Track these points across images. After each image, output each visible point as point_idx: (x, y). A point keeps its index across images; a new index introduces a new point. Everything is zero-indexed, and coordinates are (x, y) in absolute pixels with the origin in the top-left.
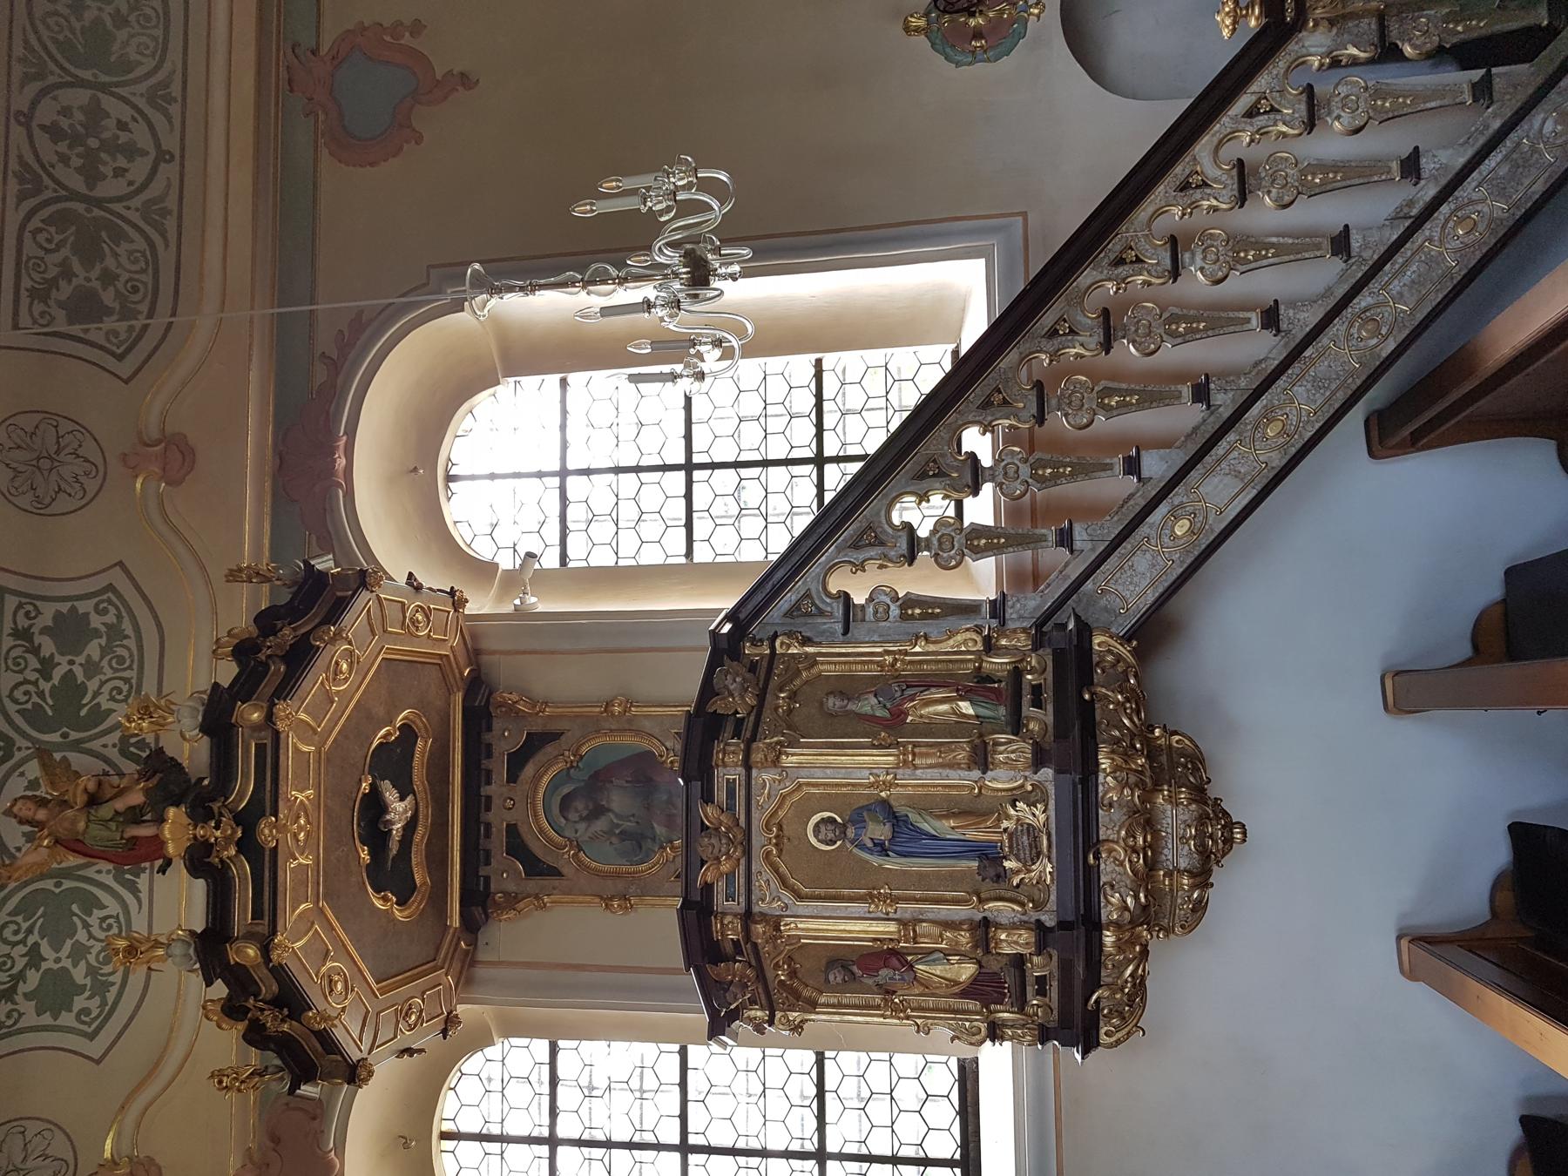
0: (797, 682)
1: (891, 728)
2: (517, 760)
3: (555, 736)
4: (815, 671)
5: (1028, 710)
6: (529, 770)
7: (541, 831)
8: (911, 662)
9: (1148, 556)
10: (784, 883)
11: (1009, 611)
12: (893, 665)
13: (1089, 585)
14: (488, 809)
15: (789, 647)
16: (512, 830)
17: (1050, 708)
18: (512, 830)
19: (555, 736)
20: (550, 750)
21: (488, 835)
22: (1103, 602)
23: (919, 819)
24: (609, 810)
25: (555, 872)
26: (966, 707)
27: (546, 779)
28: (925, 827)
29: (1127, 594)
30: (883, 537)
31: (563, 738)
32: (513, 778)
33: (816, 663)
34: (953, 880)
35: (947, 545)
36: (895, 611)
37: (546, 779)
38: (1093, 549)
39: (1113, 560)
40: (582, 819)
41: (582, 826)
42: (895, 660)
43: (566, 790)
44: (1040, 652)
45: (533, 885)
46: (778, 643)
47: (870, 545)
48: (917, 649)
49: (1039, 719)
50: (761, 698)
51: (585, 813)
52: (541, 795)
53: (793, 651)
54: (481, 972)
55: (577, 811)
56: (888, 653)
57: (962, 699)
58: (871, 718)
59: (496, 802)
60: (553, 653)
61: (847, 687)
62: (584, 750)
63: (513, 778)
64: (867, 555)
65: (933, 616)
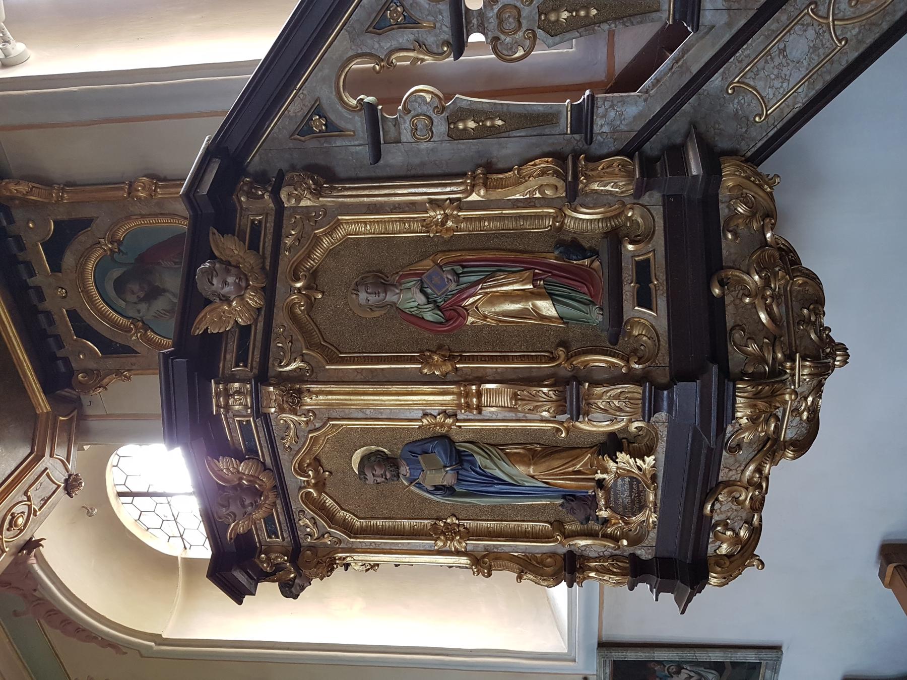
0: (318, 253)
1: (447, 347)
2: (55, 249)
3: (85, 224)
4: (340, 233)
5: (634, 311)
6: (69, 260)
7: (102, 312)
8: (466, 219)
9: (811, 33)
10: (331, 518)
11: (599, 121)
12: (443, 223)
13: (716, 81)
14: (42, 298)
15: (299, 199)
16: (73, 315)
17: (661, 302)
18: (73, 315)
19: (85, 224)
20: (83, 239)
21: (51, 322)
22: (732, 107)
23: (488, 463)
24: (165, 291)
25: (128, 350)
26: (546, 307)
27: (90, 266)
28: (498, 473)
29: (769, 93)
30: (417, 15)
31: (94, 225)
32: (56, 267)
33: (339, 223)
34: (533, 513)
35: (511, 24)
36: (441, 127)
37: (90, 266)
38: (729, 25)
39: (756, 41)
40: (141, 300)
41: (143, 307)
42: (446, 217)
43: (116, 273)
44: (646, 199)
45: (111, 363)
46: (283, 196)
47: (401, 26)
48: (474, 197)
49: (648, 320)
50: (269, 293)
51: (142, 294)
52: (91, 281)
53: (304, 203)
54: (93, 424)
55: (133, 293)
56: (436, 204)
57: (540, 297)
58: (416, 319)
59: (47, 292)
60: (54, 126)
61: (381, 267)
62: (120, 235)
63: (56, 267)
64: (394, 44)
65: (494, 132)
